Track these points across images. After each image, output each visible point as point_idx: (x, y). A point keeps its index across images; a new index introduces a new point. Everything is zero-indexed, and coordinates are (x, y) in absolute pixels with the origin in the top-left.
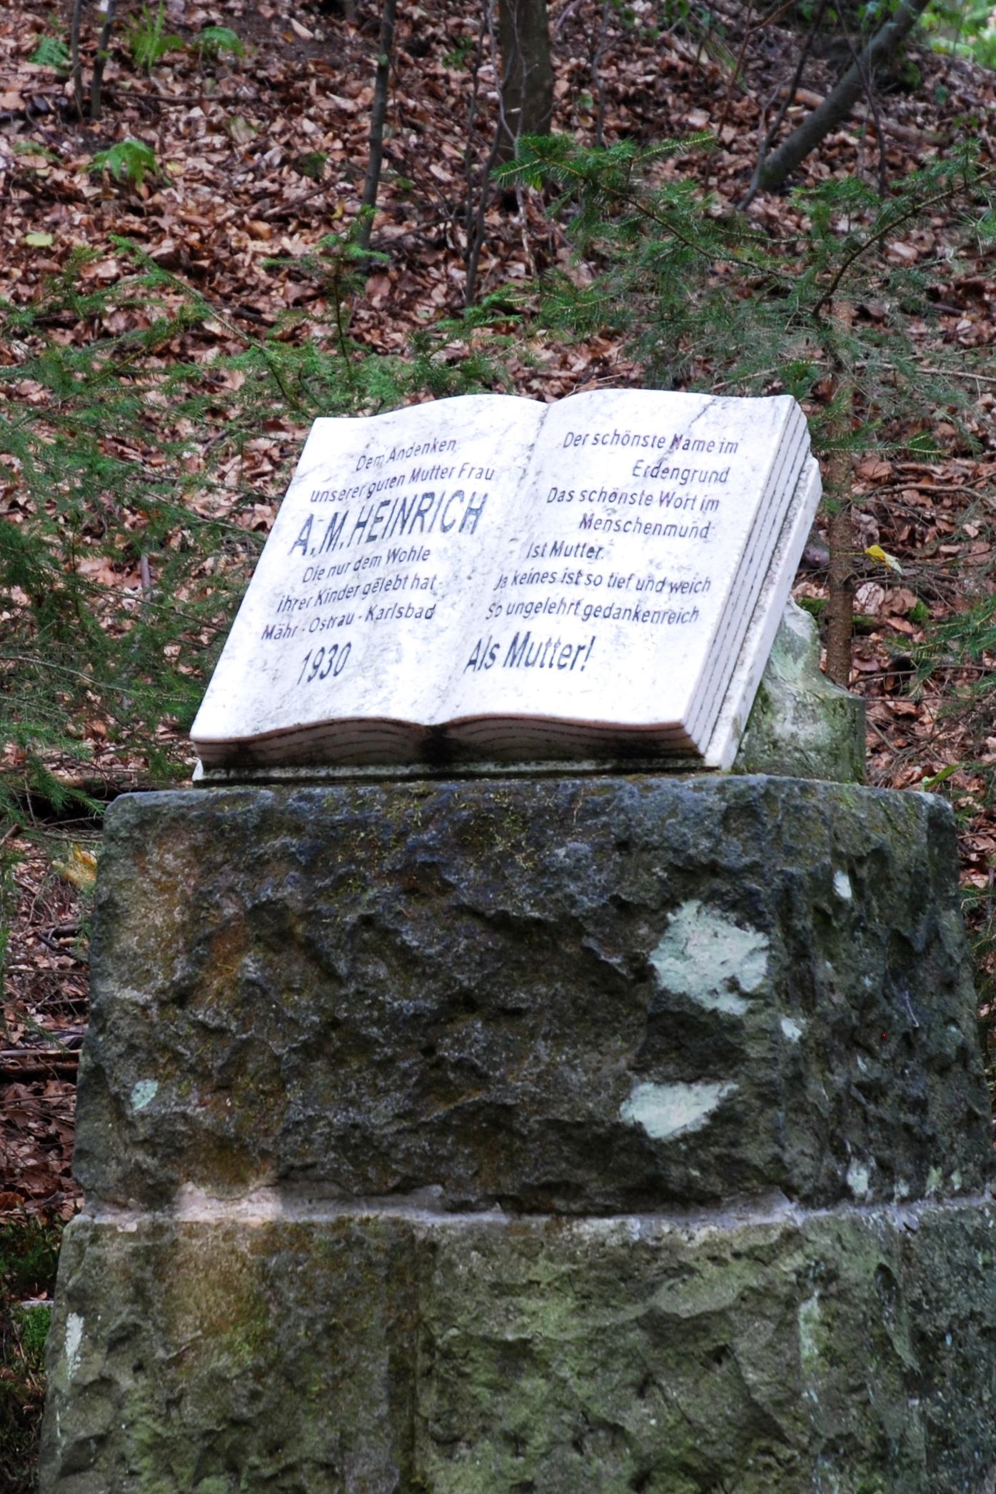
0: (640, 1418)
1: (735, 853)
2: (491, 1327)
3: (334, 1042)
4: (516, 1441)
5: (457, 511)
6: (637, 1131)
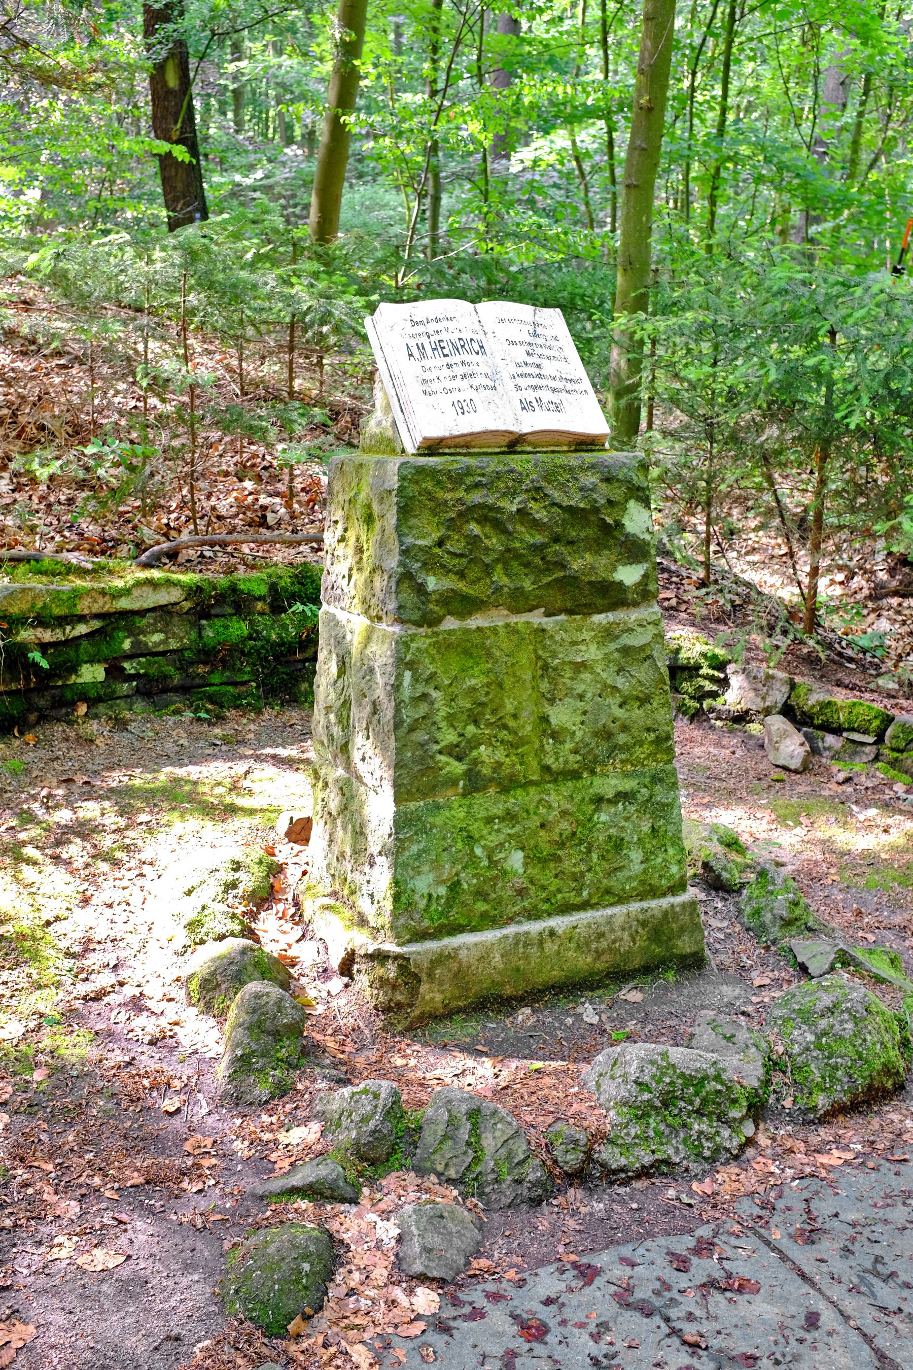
2: (571, 658)
3: (508, 556)
4: (581, 697)
5: (477, 348)
6: (621, 583)
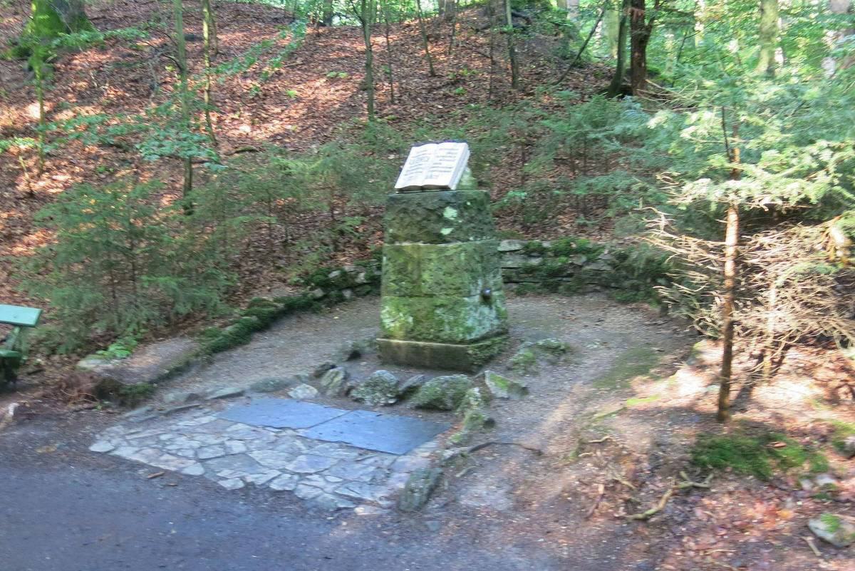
0: (444, 267)
1: (453, 200)
